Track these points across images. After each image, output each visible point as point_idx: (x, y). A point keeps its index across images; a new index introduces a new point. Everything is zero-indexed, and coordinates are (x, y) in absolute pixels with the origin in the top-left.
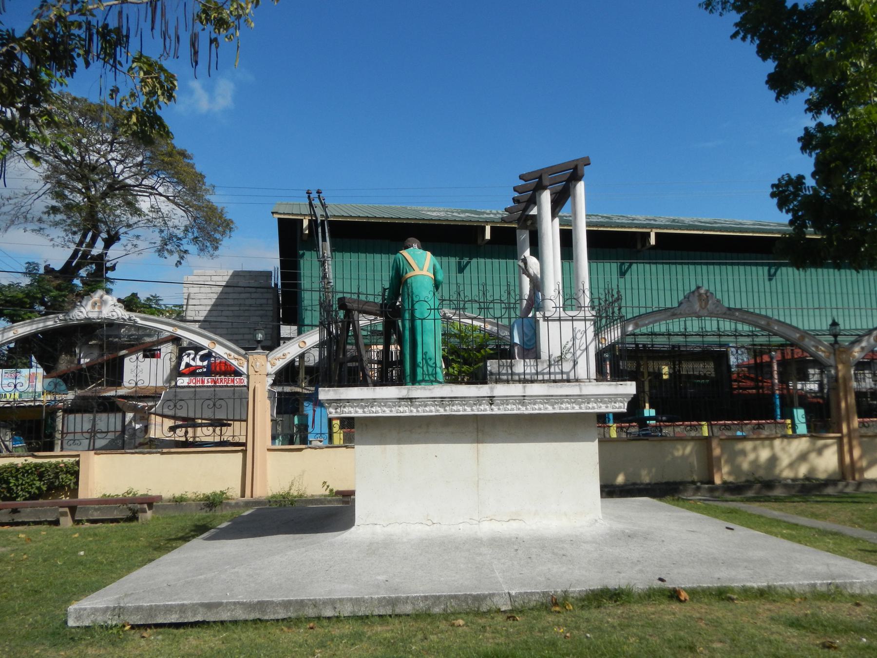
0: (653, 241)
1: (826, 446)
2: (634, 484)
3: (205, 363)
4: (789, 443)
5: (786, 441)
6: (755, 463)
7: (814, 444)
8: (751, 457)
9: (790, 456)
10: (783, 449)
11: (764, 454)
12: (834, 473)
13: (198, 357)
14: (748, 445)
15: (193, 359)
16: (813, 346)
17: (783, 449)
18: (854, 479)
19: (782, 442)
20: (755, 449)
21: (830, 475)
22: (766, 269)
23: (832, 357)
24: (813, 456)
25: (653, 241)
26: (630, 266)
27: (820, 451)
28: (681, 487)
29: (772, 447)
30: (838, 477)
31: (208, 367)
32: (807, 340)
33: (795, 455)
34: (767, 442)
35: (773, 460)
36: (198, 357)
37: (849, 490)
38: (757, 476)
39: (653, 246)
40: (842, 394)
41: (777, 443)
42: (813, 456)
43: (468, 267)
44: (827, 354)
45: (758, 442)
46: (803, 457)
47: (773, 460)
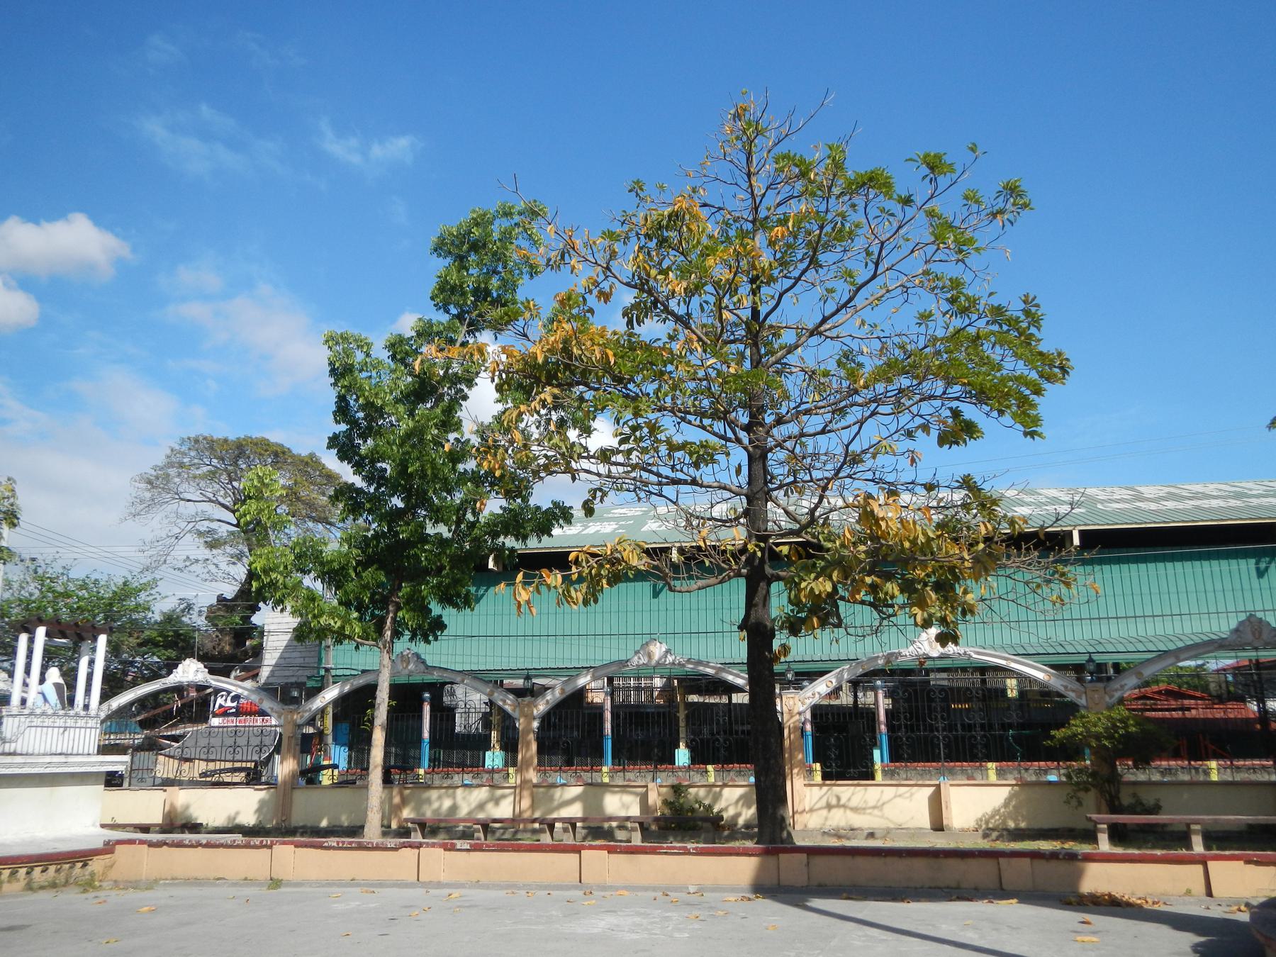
1: (504, 796)
2: (334, 826)
3: (235, 704)
4: (470, 793)
5: (468, 790)
6: (437, 811)
8: (436, 805)
9: (469, 805)
10: (464, 798)
11: (447, 803)
13: (229, 698)
14: (434, 794)
15: (226, 700)
17: (464, 798)
20: (440, 798)
23: (517, 709)
24: (490, 806)
27: (497, 801)
29: (454, 797)
31: (237, 708)
32: (496, 694)
33: (473, 805)
34: (451, 791)
35: (454, 808)
36: (229, 698)
41: (459, 792)
42: (490, 806)
43: (485, 597)
46: (481, 806)
47: (454, 808)
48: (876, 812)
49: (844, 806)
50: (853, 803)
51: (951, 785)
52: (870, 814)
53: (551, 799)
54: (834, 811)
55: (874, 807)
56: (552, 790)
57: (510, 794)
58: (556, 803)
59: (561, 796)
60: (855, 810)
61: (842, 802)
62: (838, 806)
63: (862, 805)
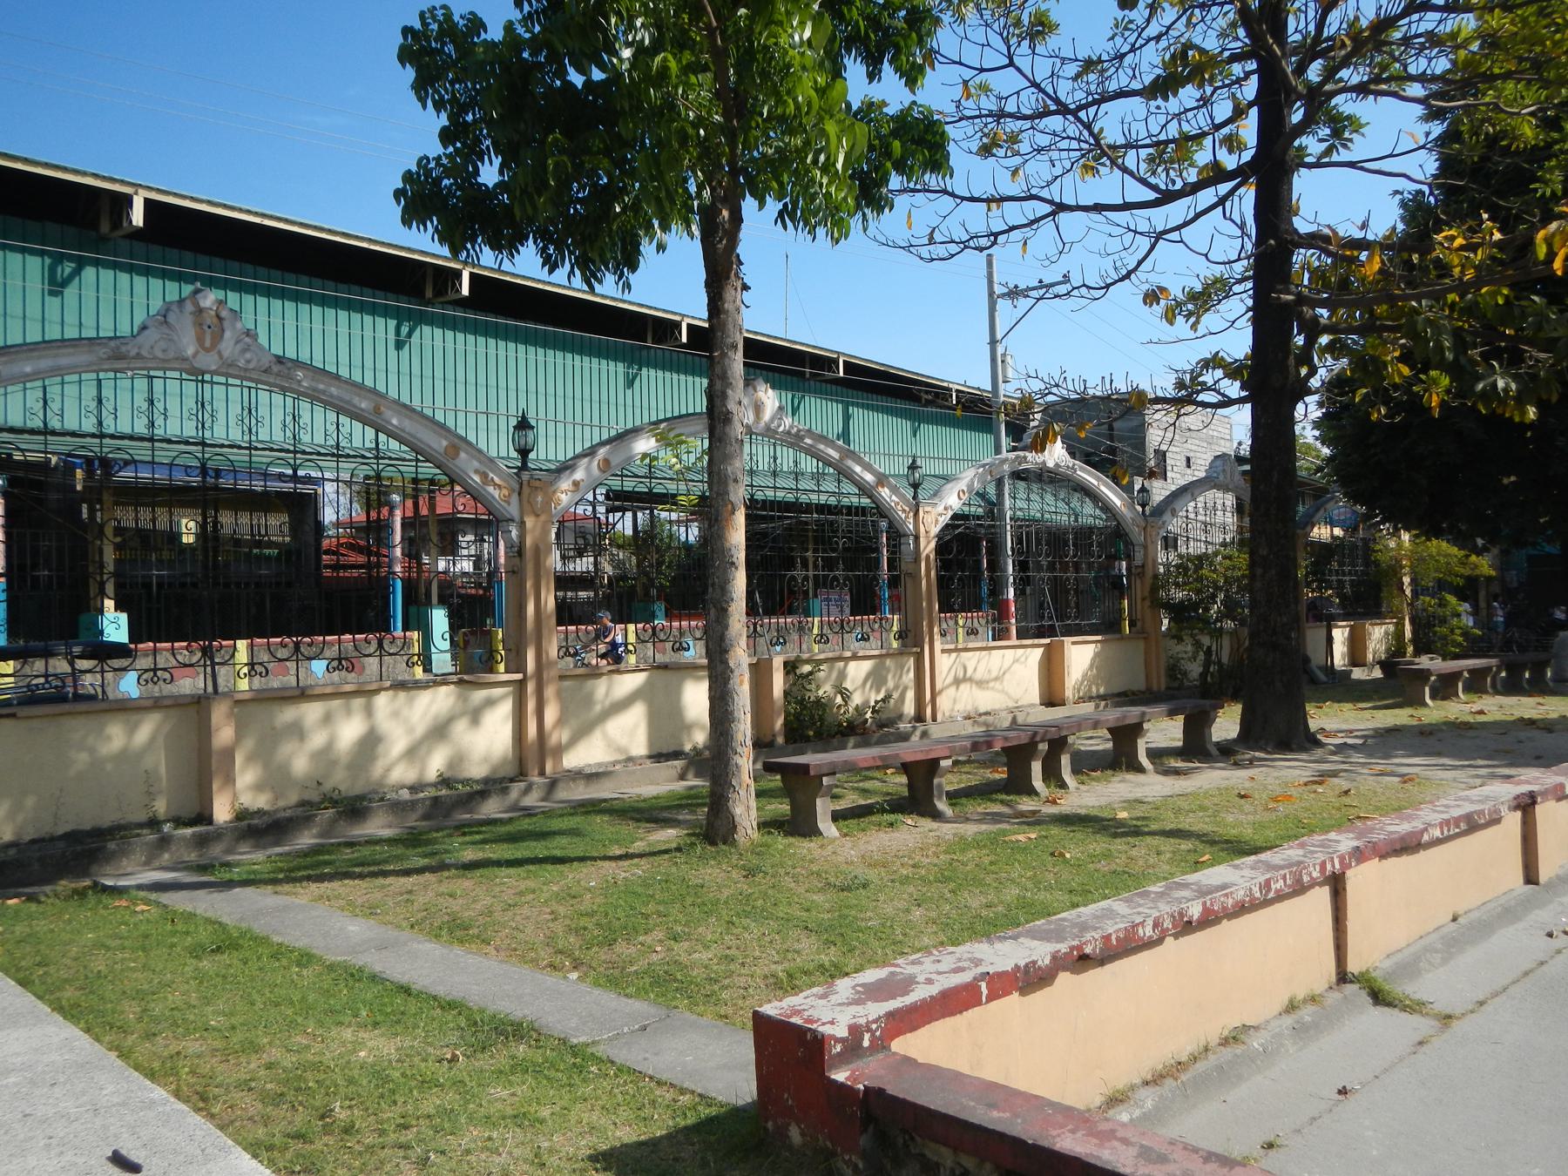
0: (138, 217)
1: (490, 703)
4: (411, 701)
5: (402, 695)
6: (325, 755)
7: (465, 700)
8: (317, 740)
9: (410, 730)
10: (396, 714)
11: (349, 731)
12: (504, 761)
16: (476, 472)
17: (396, 714)
18: (542, 773)
19: (395, 696)
20: (327, 719)
21: (495, 769)
22: (392, 323)
23: (515, 499)
24: (460, 727)
25: (138, 217)
26: (77, 272)
27: (475, 716)
28: (112, 846)
29: (369, 711)
30: (510, 771)
33: (420, 730)
34: (358, 702)
35: (371, 742)
37: (531, 800)
38: (328, 786)
39: (138, 231)
40: (529, 584)
44: (505, 492)
45: (336, 703)
46: (439, 731)
47: (371, 742)
48: (997, 685)
49: (970, 680)
50: (978, 676)
51: (1074, 643)
52: (993, 688)
53: (588, 700)
54: (962, 687)
55: (996, 679)
56: (590, 683)
57: (503, 697)
58: (598, 708)
59: (607, 694)
60: (980, 684)
61: (968, 675)
62: (965, 679)
63: (986, 677)
